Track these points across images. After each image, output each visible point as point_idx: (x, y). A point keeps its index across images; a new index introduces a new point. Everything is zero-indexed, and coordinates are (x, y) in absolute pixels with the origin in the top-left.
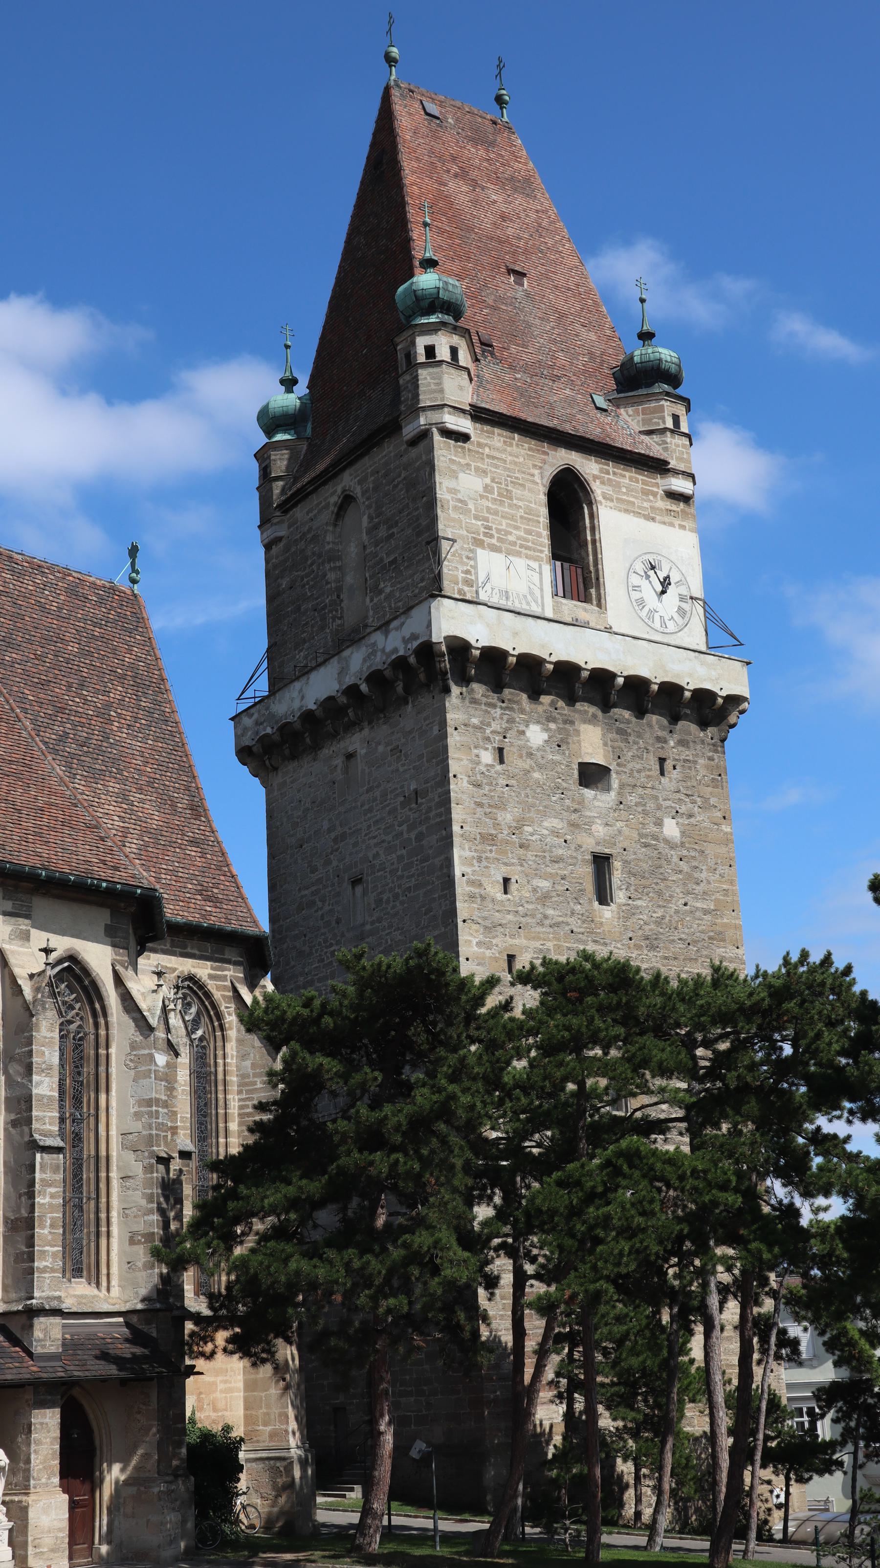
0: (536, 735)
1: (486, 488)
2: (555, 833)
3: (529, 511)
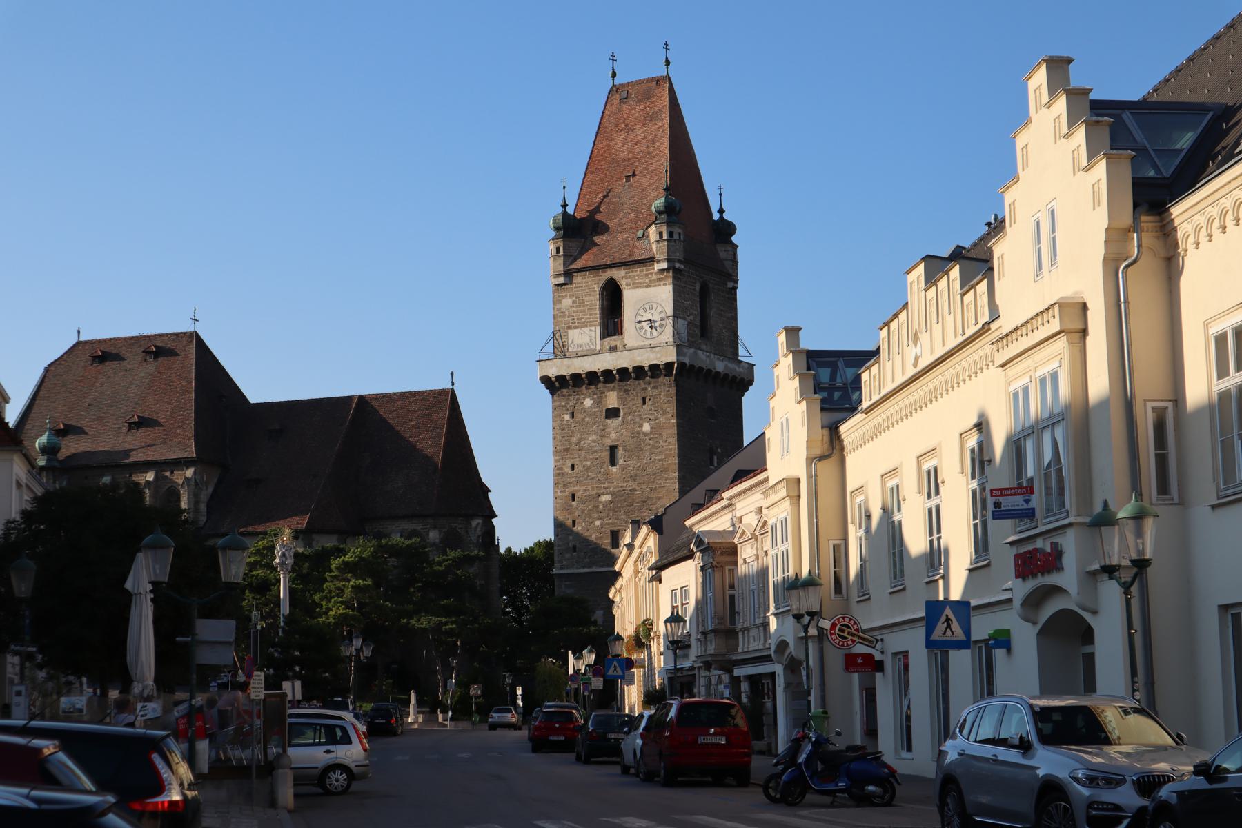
0: (588, 402)
1: (574, 302)
2: (594, 441)
3: (592, 305)
